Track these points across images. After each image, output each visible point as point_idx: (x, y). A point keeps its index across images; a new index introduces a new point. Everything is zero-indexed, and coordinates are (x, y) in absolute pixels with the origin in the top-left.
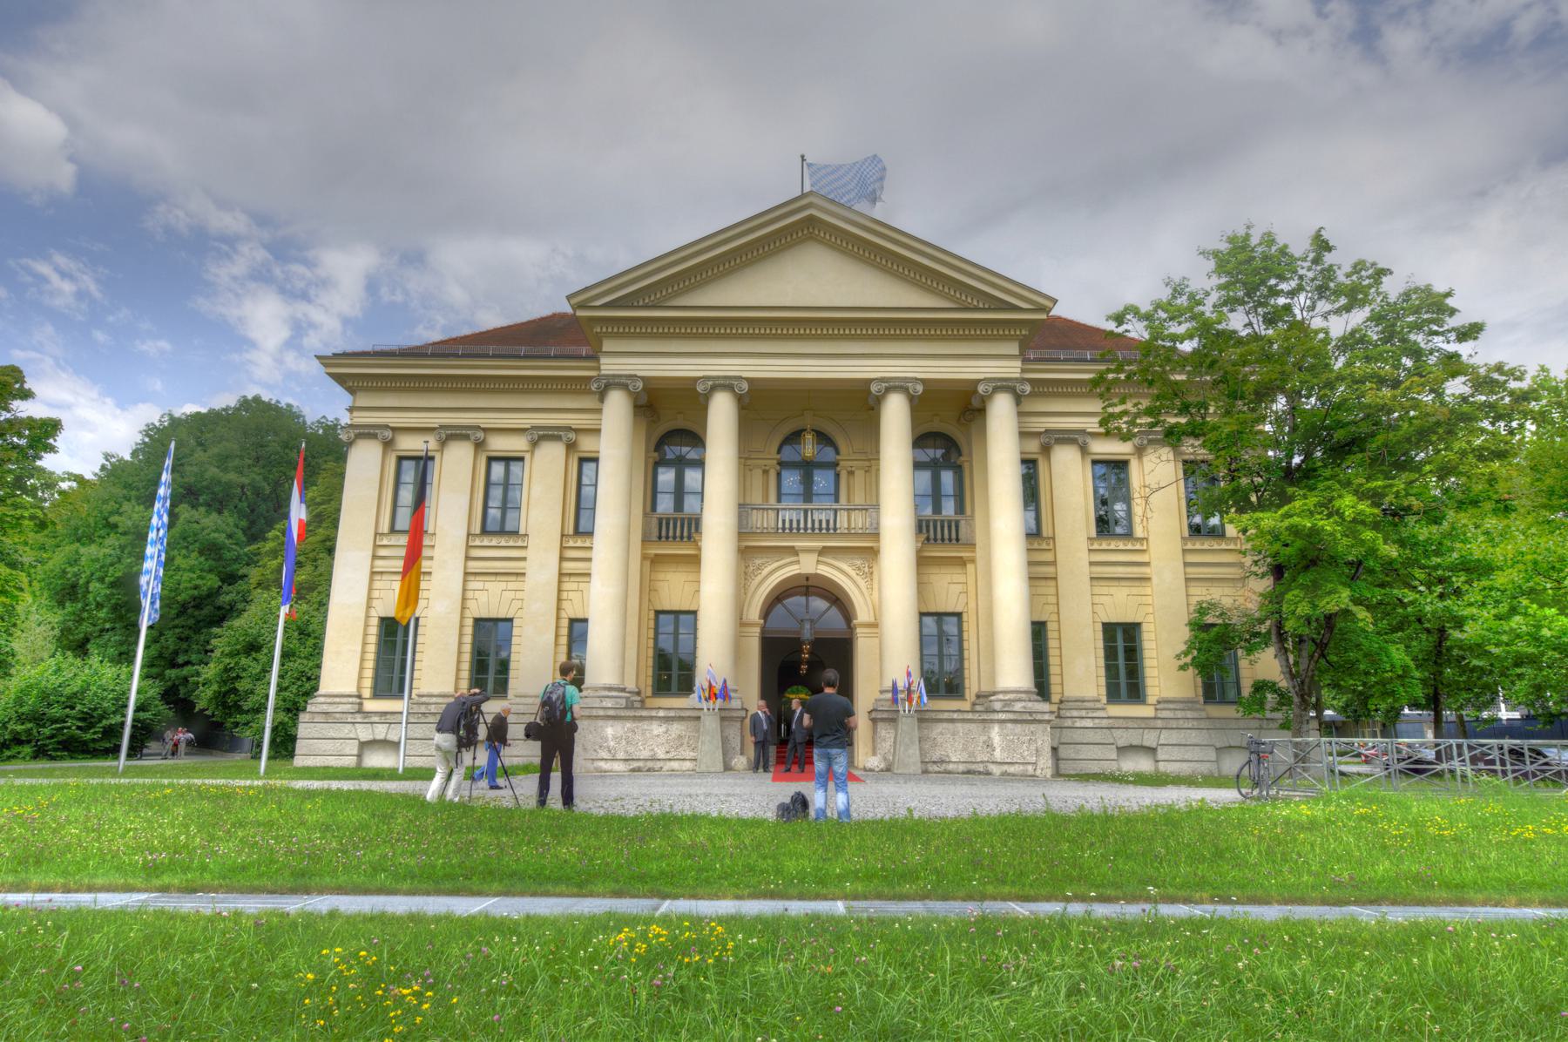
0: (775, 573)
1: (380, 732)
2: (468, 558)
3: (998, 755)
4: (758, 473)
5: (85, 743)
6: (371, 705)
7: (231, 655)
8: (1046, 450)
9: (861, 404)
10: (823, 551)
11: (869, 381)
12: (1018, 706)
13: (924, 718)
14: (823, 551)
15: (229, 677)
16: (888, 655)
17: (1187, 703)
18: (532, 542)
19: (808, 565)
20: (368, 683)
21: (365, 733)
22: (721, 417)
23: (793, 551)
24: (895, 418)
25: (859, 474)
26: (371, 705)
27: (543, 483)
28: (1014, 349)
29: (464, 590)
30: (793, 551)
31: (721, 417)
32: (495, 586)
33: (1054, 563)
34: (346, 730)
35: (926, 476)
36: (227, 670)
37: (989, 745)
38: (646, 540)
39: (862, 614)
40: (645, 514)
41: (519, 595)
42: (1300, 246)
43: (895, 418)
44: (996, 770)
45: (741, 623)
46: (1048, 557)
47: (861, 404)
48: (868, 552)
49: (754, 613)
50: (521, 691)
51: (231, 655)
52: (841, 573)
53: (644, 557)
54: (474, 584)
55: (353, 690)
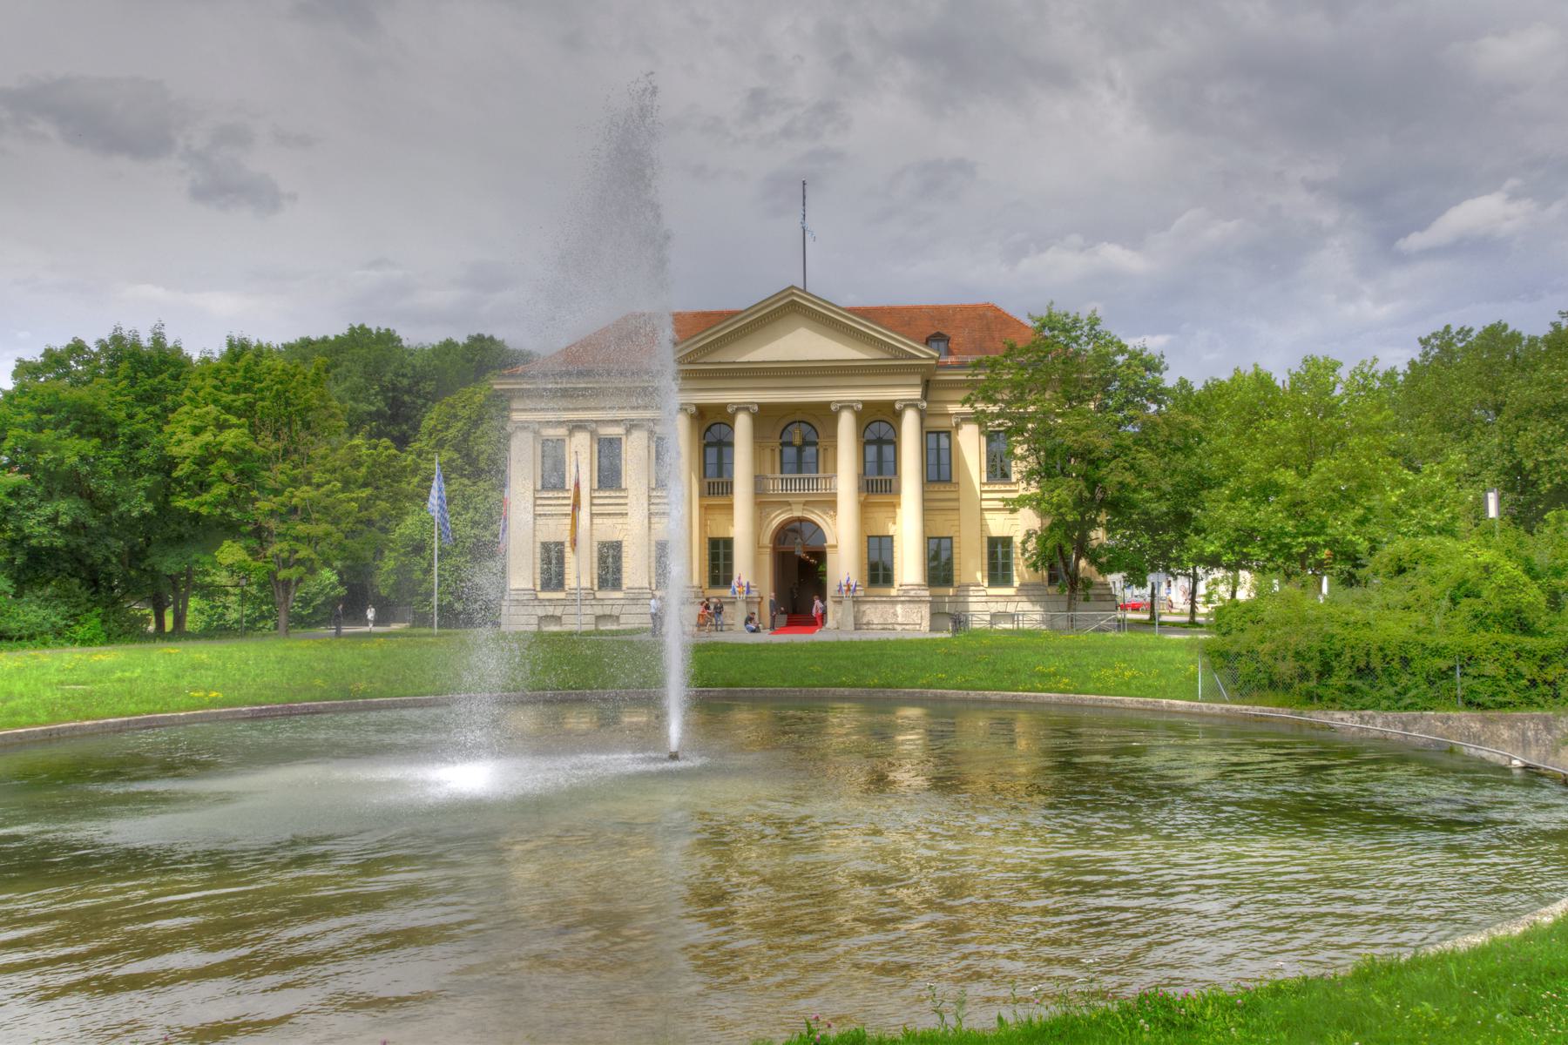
0: (778, 518)
1: (550, 611)
3: (900, 620)
4: (768, 452)
5: (302, 617)
6: (542, 595)
7: (405, 554)
8: (958, 426)
9: (825, 416)
10: (806, 504)
11: (829, 403)
13: (857, 602)
14: (806, 504)
15: (403, 571)
16: (844, 565)
17: (1035, 586)
18: (631, 493)
19: (797, 513)
20: (538, 582)
21: (541, 612)
22: (743, 425)
23: (788, 503)
24: (846, 426)
26: (542, 595)
27: (634, 450)
28: (917, 380)
30: (788, 503)
31: (743, 425)
32: (609, 521)
33: (957, 500)
35: (872, 450)
36: (403, 565)
37: (895, 614)
38: (701, 496)
39: (830, 541)
40: (700, 481)
42: (1084, 316)
43: (846, 426)
44: (899, 628)
45: (757, 545)
46: (953, 496)
47: (825, 416)
48: (830, 504)
49: (767, 539)
51: (405, 554)
52: (815, 516)
53: (701, 506)
54: (597, 520)
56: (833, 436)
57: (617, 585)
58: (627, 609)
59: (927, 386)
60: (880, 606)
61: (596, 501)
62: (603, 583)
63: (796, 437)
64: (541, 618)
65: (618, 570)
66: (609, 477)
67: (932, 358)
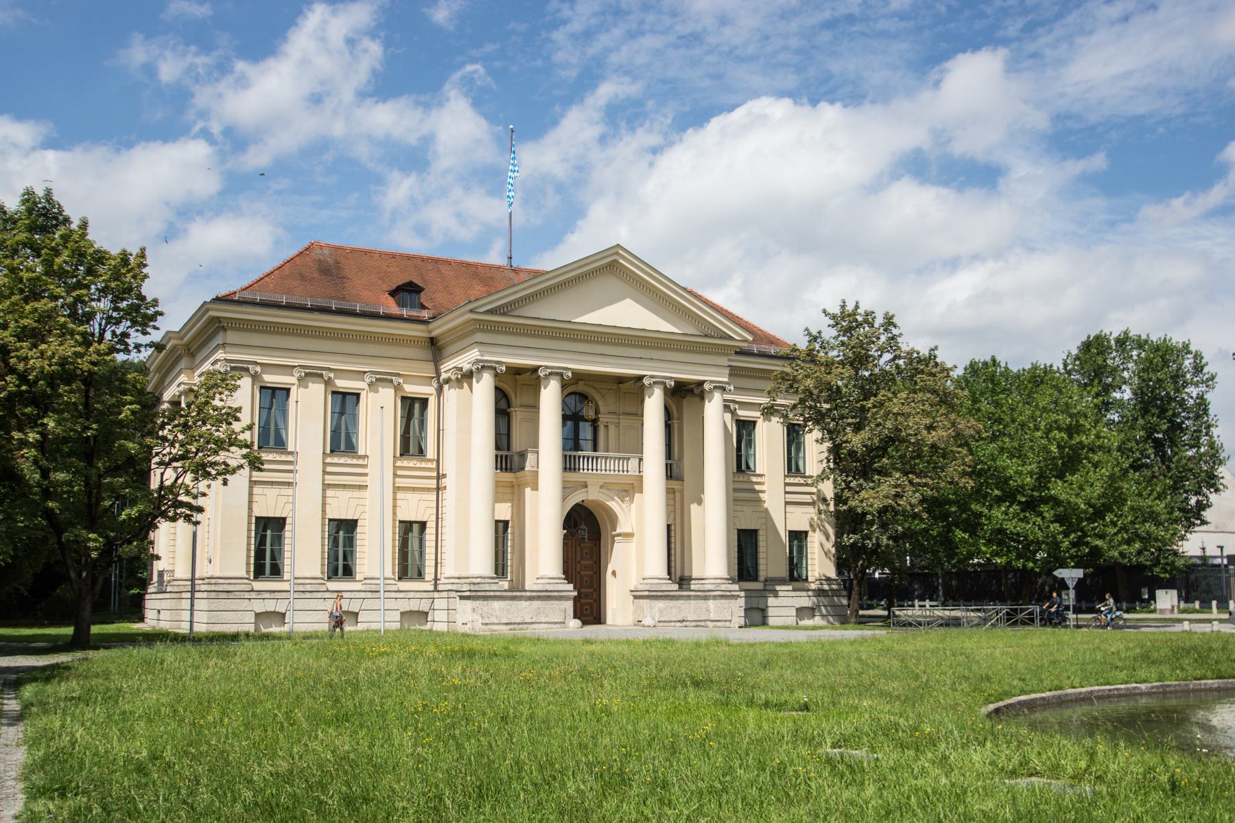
1: (270, 606)
2: (325, 473)
12: (723, 587)
21: (260, 607)
25: (612, 428)
29: (324, 497)
34: (244, 604)
41: (361, 502)
50: (367, 575)
55: (244, 574)
56: (535, 407)
57: (348, 572)
58: (368, 604)
59: (735, 372)
60: (680, 603)
61: (329, 469)
62: (333, 574)
63: (594, 410)
64: (257, 615)
65: (349, 555)
66: (342, 440)
67: (746, 341)
